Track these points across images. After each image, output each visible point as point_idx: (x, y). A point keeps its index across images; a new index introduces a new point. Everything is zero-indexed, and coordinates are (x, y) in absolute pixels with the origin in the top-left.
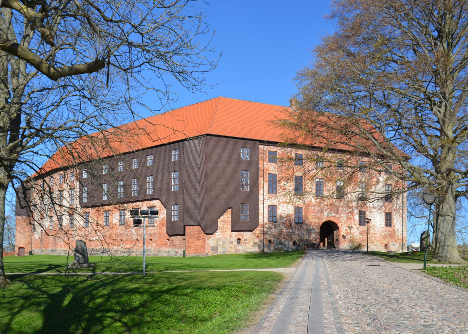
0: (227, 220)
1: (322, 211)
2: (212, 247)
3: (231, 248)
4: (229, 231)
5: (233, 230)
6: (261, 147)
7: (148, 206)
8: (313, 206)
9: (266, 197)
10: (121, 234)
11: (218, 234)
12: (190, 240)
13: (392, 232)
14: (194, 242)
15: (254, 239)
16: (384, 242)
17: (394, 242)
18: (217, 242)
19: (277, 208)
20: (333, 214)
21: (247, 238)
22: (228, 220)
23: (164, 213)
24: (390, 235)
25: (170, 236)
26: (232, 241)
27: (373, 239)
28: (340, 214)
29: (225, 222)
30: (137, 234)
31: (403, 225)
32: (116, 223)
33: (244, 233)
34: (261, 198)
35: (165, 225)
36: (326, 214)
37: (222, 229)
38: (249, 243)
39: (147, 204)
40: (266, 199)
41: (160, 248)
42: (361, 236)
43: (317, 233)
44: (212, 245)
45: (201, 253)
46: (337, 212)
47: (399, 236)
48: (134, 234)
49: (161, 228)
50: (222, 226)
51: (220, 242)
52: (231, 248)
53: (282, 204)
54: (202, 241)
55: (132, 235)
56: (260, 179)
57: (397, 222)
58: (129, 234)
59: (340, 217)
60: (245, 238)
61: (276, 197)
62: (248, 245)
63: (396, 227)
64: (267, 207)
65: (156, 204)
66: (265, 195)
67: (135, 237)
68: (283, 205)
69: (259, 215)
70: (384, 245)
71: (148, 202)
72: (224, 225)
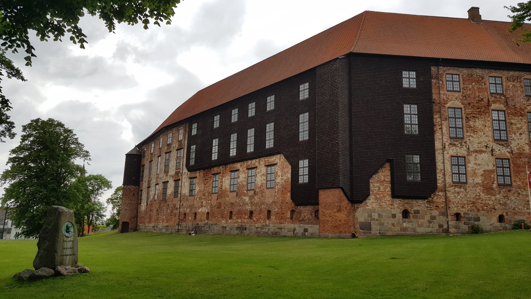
0: (384, 180)
4: (388, 198)
6: (433, 69)
7: (267, 164)
8: (526, 157)
9: (447, 144)
10: (232, 204)
11: (371, 203)
14: (332, 214)
15: (430, 212)
18: (370, 216)
22: (387, 180)
23: (287, 173)
25: (297, 205)
26: (393, 212)
30: (251, 203)
32: (226, 188)
34: (438, 145)
35: (290, 189)
37: (376, 193)
38: (423, 218)
39: (265, 161)
40: (447, 147)
41: (281, 224)
48: (247, 204)
49: (283, 193)
53: (474, 155)
54: (346, 212)
55: (245, 204)
56: (435, 117)
58: (241, 204)
60: (416, 209)
62: (421, 221)
65: (277, 161)
66: (444, 140)
67: (249, 208)
68: (476, 156)
69: (438, 171)
71: (266, 159)
72: (379, 187)
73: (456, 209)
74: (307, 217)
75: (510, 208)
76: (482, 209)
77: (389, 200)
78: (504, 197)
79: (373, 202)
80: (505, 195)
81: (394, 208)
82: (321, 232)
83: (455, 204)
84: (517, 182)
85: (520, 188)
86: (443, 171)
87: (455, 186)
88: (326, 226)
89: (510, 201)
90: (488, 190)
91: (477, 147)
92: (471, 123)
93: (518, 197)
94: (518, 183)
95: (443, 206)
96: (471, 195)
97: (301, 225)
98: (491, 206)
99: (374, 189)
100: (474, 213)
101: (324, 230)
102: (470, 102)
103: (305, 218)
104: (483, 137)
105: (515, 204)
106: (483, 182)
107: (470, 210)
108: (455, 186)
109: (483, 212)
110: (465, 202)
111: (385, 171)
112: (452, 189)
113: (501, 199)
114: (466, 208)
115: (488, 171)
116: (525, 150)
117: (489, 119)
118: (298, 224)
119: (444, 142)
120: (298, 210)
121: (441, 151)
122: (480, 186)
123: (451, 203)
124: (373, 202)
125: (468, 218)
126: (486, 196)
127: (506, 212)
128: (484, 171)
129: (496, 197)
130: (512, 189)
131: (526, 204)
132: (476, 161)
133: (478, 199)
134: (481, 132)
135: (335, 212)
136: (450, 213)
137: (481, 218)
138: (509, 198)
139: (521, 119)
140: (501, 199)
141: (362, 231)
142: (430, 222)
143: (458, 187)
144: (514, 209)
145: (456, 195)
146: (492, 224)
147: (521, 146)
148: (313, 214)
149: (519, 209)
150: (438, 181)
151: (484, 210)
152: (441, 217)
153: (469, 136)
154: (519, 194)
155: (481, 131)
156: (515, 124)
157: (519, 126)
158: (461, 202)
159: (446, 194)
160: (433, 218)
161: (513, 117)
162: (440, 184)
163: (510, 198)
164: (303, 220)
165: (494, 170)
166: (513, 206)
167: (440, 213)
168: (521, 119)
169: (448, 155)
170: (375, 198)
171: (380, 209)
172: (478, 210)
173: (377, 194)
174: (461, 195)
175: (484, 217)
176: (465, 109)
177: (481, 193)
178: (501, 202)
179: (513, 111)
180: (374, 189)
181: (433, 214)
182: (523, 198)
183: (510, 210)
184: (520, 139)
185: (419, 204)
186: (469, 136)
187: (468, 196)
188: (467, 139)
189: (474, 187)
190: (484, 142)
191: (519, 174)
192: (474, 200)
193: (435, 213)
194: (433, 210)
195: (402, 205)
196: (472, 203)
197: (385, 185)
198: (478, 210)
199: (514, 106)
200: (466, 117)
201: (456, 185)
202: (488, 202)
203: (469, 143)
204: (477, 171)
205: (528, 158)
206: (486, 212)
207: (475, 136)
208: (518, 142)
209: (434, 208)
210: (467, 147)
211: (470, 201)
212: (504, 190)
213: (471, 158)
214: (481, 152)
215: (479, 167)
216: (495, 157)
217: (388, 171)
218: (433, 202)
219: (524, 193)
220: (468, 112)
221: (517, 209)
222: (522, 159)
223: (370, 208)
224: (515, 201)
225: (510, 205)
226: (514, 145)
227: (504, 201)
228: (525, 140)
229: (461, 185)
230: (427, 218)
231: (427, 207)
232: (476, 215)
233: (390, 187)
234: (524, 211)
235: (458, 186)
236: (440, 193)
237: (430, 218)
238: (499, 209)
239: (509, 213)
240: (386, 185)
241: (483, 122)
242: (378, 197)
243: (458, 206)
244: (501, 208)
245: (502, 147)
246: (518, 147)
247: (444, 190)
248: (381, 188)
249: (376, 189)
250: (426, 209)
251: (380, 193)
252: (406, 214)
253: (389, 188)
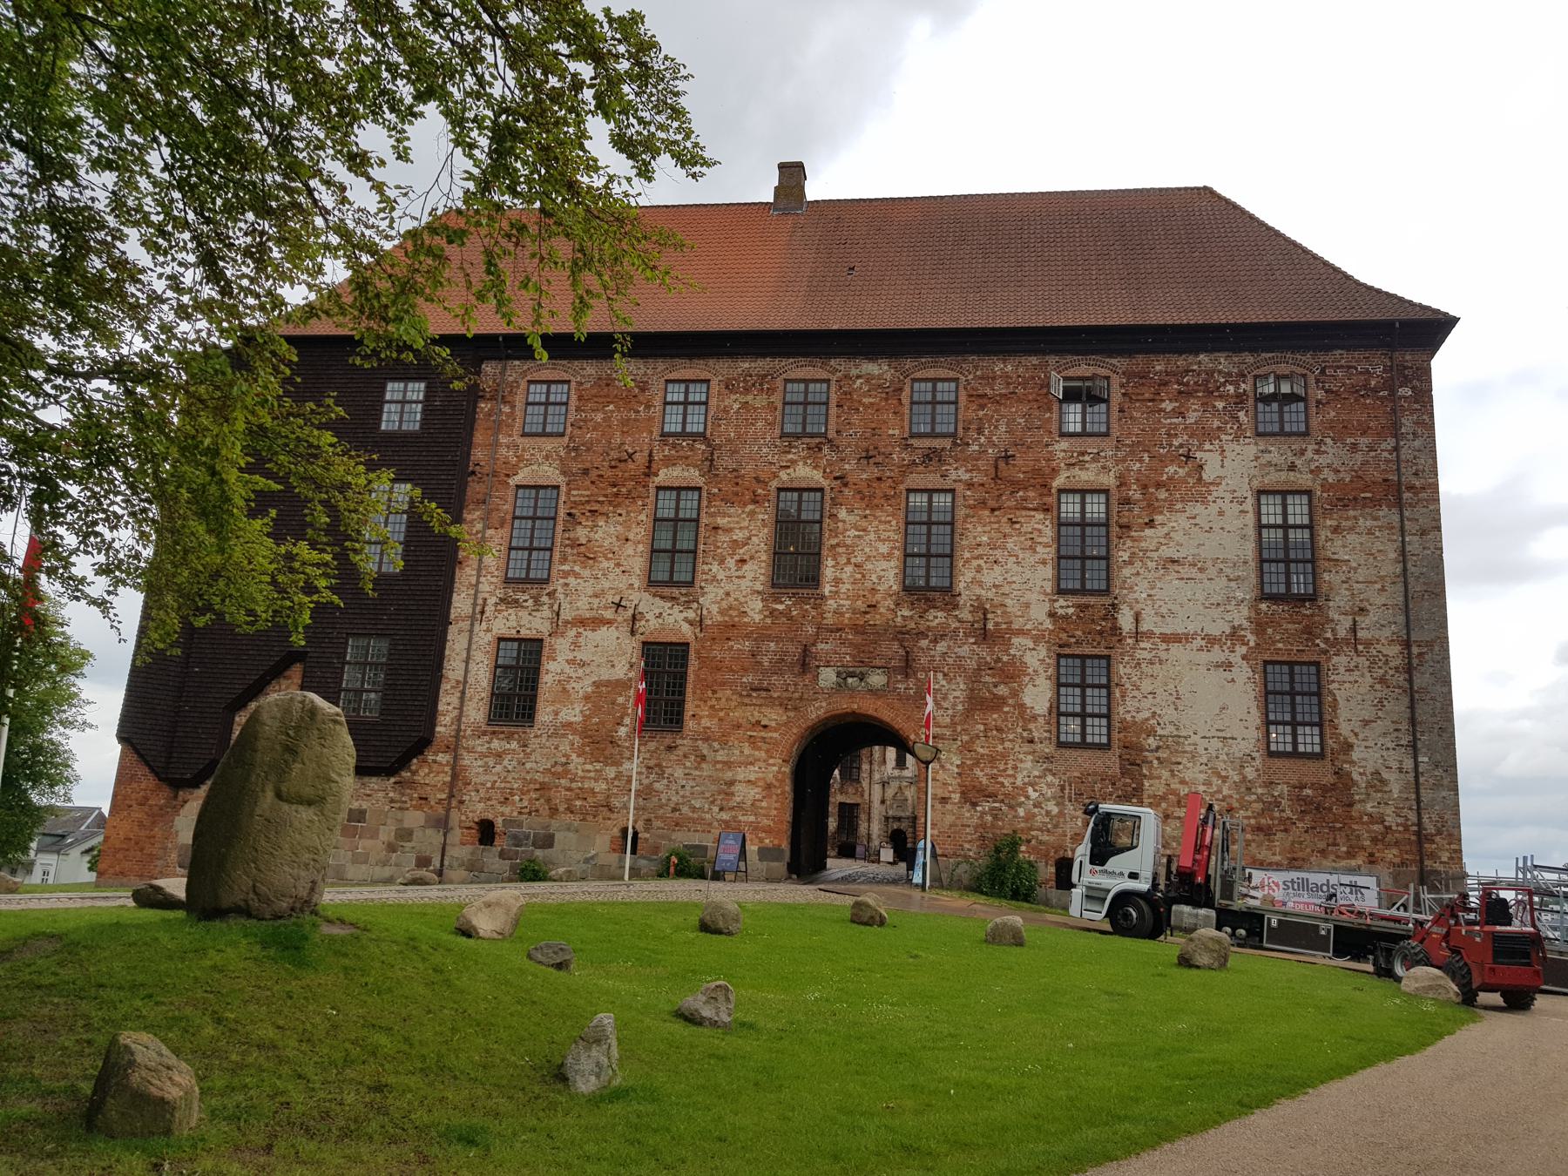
53: (573, 633)
64: (492, 649)
76: (568, 809)
80: (652, 763)
83: (482, 793)
85: (706, 740)
87: (494, 733)
90: (599, 744)
94: (706, 722)
96: (538, 763)
98: (600, 797)
100: (540, 819)
108: (494, 733)
109: (568, 818)
115: (608, 683)
122: (575, 732)
123: (470, 787)
125: (515, 837)
126: (588, 767)
129: (621, 769)
131: (719, 793)
133: (559, 776)
136: (461, 821)
137: (558, 836)
138: (664, 772)
149: (694, 809)
151: (572, 812)
154: (703, 758)
158: (503, 785)
159: (455, 758)
172: (554, 811)
174: (506, 762)
175: (567, 833)
177: (574, 756)
187: (528, 766)
189: (555, 734)
198: (554, 811)
202: (593, 784)
211: (533, 781)
213: (562, 646)
218: (411, 784)
221: (685, 809)
227: (646, 782)
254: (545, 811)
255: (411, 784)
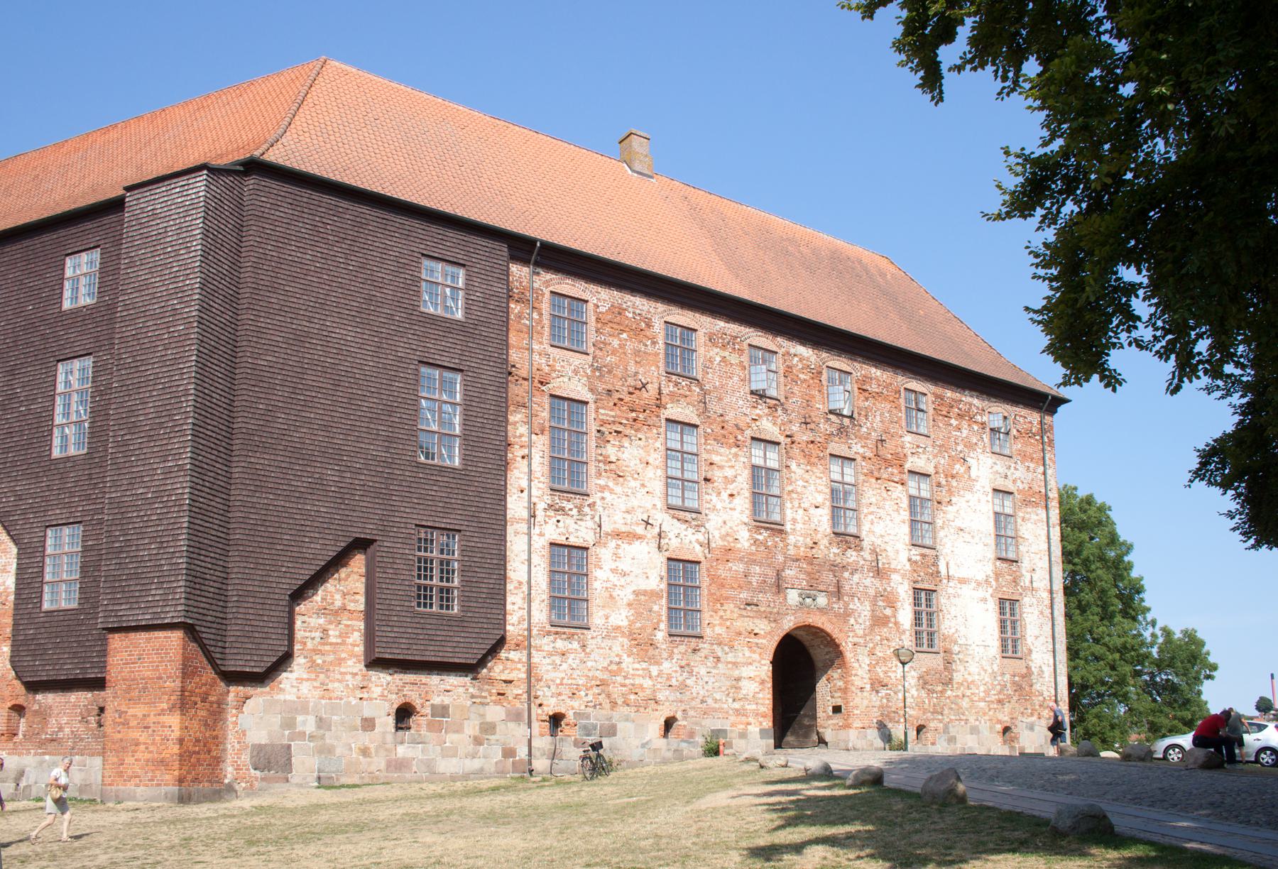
0: (344, 609)
1: (779, 586)
2: (259, 749)
3: (365, 752)
4: (355, 665)
5: (376, 663)
8: (741, 560)
11: (292, 682)
12: (131, 712)
13: (1023, 677)
14: (152, 719)
15: (481, 709)
16: (1001, 716)
17: (1032, 715)
18: (289, 724)
19: (592, 560)
20: (822, 600)
21: (447, 700)
22: (351, 606)
24: (1019, 688)
25: (34, 687)
26: (367, 714)
27: (965, 703)
28: (846, 598)
29: (336, 614)
31: (1054, 652)
33: (434, 680)
34: (516, 506)
35: (9, 630)
36: (793, 596)
37: (314, 650)
38: (459, 730)
40: (540, 514)
42: (923, 694)
43: (763, 682)
44: (258, 736)
45: (196, 780)
46: (838, 592)
47: (1046, 694)
50: (318, 634)
51: (307, 724)
52: (365, 752)
54: (203, 713)
56: (511, 418)
57: (1037, 637)
59: (847, 614)
60: (437, 700)
61: (587, 509)
62: (451, 738)
63: (1034, 656)
64: (546, 552)
66: (534, 492)
68: (618, 547)
69: (510, 587)
70: (999, 727)
72: (325, 631)
73: (553, 701)
74: (67, 730)
75: (693, 699)
76: (624, 702)
77: (356, 674)
78: (682, 667)
79: (302, 679)
80: (683, 663)
81: (371, 699)
82: (108, 780)
83: (553, 689)
84: (714, 626)
85: (719, 644)
86: (525, 588)
87: (557, 633)
88: (129, 760)
89: (694, 678)
90: (642, 645)
91: (623, 521)
92: (611, 451)
93: (714, 667)
94: (718, 630)
95: (520, 692)
96: (597, 661)
97: (47, 757)
98: (648, 692)
99: (308, 634)
100: (604, 712)
101: (120, 774)
102: (610, 388)
103: (61, 735)
104: (639, 495)
105: (706, 687)
106: (632, 623)
107: (592, 704)
108: (557, 633)
109: (625, 710)
110: (580, 682)
111: (346, 579)
112: (546, 643)
113: (674, 674)
114: (580, 698)
115: (645, 593)
116: (741, 540)
117: (658, 445)
118: (36, 754)
119: (534, 500)
120: (36, 707)
121: (523, 527)
123: (542, 684)
124: (300, 680)
125: (585, 727)
126: (637, 666)
127: (683, 708)
128: (636, 593)
129: (661, 668)
130: (701, 645)
132: (617, 564)
133: (614, 673)
134: (635, 479)
135: (162, 712)
136: (537, 715)
137: (621, 726)
139: (736, 455)
140: (674, 674)
141: (258, 772)
142: (478, 741)
143: (564, 636)
144: (703, 702)
145: (558, 662)
146: (647, 743)
147: (731, 528)
148: (92, 719)
149: (716, 701)
150: (508, 617)
151: (628, 705)
152: (511, 725)
153: (603, 489)
154: (718, 659)
155: (636, 476)
156: (721, 467)
157: (729, 473)
158: (570, 682)
159: (529, 655)
160: (488, 728)
161: (717, 447)
162: (514, 627)
163: (696, 670)
164: (53, 740)
165: (662, 590)
166: (702, 693)
167: (508, 714)
168: (736, 455)
169: (542, 538)
170: (309, 665)
171: (323, 702)
173: (316, 651)
174: (570, 661)
176: (598, 408)
177: (625, 656)
178: (674, 682)
179: (718, 430)
180: (308, 634)
181: (489, 719)
182: (727, 672)
183: (693, 703)
184: (731, 509)
185: (449, 688)
186: (603, 489)
187: (589, 664)
188: (596, 497)
189: (607, 637)
190: (641, 510)
191: (722, 605)
192: (605, 677)
193: (495, 713)
194: (488, 704)
195: (395, 689)
196: (598, 683)
197: (345, 622)
198: (614, 704)
199: (722, 415)
200: (599, 431)
201: (559, 629)
203: (601, 509)
204: (619, 592)
205: (746, 563)
206: (634, 709)
207: (618, 489)
208: (725, 517)
209: (494, 698)
210: (597, 519)
212: (682, 648)
213: (604, 554)
214: (632, 537)
215: (623, 580)
216: (667, 554)
217: (356, 577)
218: (490, 681)
219: (730, 657)
220: (604, 418)
221: (710, 701)
222: (730, 565)
223: (288, 697)
224: (706, 679)
225: (694, 691)
226: (714, 523)
227: (680, 679)
228: (742, 512)
229: (573, 630)
230: (471, 728)
231: (473, 696)
232: (607, 719)
233: (359, 630)
234: (726, 706)
235: (564, 633)
236: (513, 655)
237: (480, 728)
238: (667, 700)
239: (691, 713)
240: (349, 623)
241: (641, 451)
242: (319, 661)
243: (560, 694)
244: (671, 698)
245: (684, 526)
246: (723, 531)
247: (526, 644)
248: (331, 633)
249: (313, 634)
250: (469, 703)
251: (327, 648)
252: (404, 714)
253: (356, 634)
254: (607, 706)
255: (490, 681)
